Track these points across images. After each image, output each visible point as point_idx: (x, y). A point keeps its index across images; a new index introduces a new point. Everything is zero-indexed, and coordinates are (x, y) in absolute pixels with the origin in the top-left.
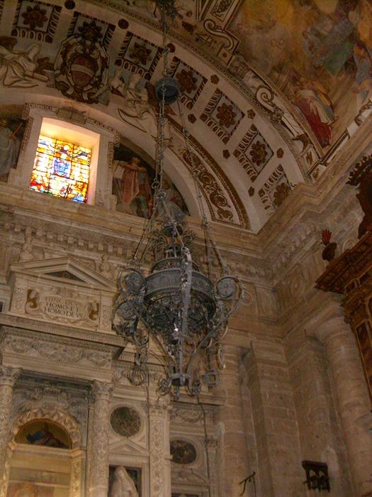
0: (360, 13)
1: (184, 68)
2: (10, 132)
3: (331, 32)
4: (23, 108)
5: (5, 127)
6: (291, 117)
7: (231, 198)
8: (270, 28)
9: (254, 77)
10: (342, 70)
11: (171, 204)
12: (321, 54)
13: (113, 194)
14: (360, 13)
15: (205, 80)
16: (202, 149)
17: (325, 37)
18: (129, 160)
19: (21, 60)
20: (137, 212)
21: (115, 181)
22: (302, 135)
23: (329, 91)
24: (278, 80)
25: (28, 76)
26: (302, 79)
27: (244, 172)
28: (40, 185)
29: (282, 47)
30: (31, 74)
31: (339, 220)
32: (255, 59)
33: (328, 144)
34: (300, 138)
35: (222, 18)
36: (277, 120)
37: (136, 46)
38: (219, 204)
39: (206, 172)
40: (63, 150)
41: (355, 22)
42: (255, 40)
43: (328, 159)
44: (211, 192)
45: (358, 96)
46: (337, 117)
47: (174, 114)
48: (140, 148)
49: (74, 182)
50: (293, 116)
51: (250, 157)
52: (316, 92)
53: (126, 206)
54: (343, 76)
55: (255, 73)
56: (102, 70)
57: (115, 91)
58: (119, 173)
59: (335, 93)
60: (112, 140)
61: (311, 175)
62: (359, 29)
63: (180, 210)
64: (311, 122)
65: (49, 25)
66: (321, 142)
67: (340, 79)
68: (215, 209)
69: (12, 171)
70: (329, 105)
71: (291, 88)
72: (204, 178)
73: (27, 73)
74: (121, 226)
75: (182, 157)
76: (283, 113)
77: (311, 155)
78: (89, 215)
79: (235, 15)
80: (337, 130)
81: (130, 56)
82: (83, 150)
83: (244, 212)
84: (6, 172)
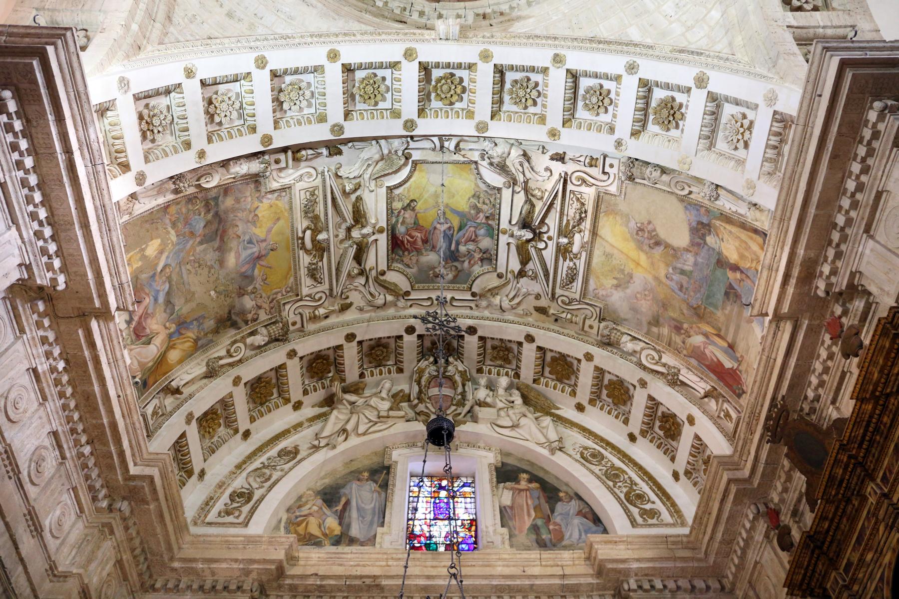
0: (718, 235)
1: (553, 354)
2: (374, 486)
3: (696, 264)
4: (385, 452)
5: (367, 480)
7: (653, 491)
8: (629, 282)
9: (631, 340)
10: (724, 302)
11: (577, 521)
13: (502, 526)
14: (718, 235)
15: (579, 361)
16: (602, 440)
17: (691, 272)
18: (516, 480)
19: (374, 401)
20: (538, 543)
21: (503, 511)
23: (719, 330)
24: (659, 335)
25: (383, 417)
26: (685, 326)
27: (660, 453)
28: (420, 536)
30: (385, 414)
31: (785, 490)
32: (625, 320)
33: (744, 392)
35: (574, 290)
36: (675, 381)
37: (494, 348)
38: (638, 502)
39: (613, 466)
40: (441, 488)
41: (716, 247)
42: (617, 300)
44: (625, 490)
47: (558, 409)
48: (528, 461)
49: (459, 523)
51: (661, 433)
52: (706, 335)
53: (524, 537)
54: (729, 308)
56: (464, 385)
57: (482, 404)
58: (507, 498)
59: (727, 329)
60: (492, 461)
63: (591, 524)
64: (714, 371)
65: (396, 357)
66: (734, 392)
67: (727, 312)
68: (635, 511)
69: (380, 530)
70: (726, 345)
71: (677, 339)
72: (612, 476)
73: (383, 414)
74: (512, 568)
75: (578, 457)
76: (679, 371)
77: (728, 411)
78: (470, 564)
79: (586, 281)
80: (746, 371)
81: (491, 360)
82: (464, 480)
83: (674, 504)
84: (373, 534)
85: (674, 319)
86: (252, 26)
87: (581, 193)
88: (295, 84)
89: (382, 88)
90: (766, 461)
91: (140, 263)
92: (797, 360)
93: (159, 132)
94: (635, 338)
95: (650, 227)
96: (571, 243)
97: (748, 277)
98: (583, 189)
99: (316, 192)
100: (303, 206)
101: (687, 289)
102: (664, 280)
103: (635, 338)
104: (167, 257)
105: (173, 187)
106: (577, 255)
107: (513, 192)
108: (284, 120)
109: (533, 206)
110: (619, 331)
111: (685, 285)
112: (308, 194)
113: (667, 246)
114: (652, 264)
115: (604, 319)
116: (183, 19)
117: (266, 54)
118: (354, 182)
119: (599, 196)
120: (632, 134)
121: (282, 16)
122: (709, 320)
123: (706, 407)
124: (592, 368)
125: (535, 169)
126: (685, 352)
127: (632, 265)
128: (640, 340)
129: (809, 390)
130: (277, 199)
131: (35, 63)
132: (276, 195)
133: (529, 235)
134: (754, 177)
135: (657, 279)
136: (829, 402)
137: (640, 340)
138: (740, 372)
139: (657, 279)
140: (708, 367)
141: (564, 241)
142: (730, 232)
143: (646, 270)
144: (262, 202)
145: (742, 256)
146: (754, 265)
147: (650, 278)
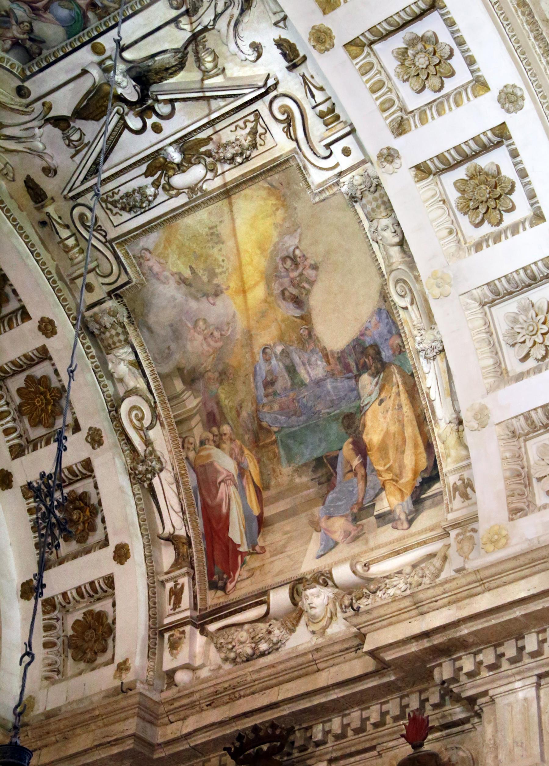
0: (381, 390)
3: (319, 383)
6: (174, 487)
8: (206, 295)
9: (131, 363)
12: (282, 408)
14: (381, 390)
17: (303, 384)
22: (179, 537)
26: (226, 429)
27: (31, 538)
29: (212, 343)
33: (224, 588)
34: (172, 539)
35: (117, 220)
41: (366, 400)
43: (211, 622)
45: (316, 537)
46: (263, 548)
50: (178, 487)
52: (242, 471)
54: (305, 479)
55: (137, 356)
61: (166, 635)
62: (369, 414)
64: (207, 521)
66: (211, 574)
67: (297, 480)
70: (256, 512)
76: (161, 470)
80: (252, 573)
85: (218, 403)
87: (267, 129)
90: (196, 745)
92: (343, 697)
94: (138, 364)
95: (310, 273)
96: (180, 168)
97: (365, 478)
98: (277, 130)
101: (275, 393)
102: (257, 350)
103: (138, 364)
106: (172, 188)
107: (175, 21)
109: (181, 66)
110: (126, 333)
111: (279, 386)
113: (306, 319)
114: (263, 314)
115: (118, 296)
119: (287, 161)
120: (418, 167)
122: (265, 459)
123: (156, 554)
124: (38, 344)
125: (240, 28)
126: (192, 455)
127: (233, 284)
128: (144, 375)
129: (320, 727)
133: (132, 95)
134: (497, 416)
135: (249, 336)
136: (328, 757)
137: (144, 375)
138: (243, 562)
139: (249, 336)
140: (205, 508)
141: (176, 156)
142: (400, 407)
143: (247, 310)
145: (383, 448)
146: (387, 476)
147: (240, 325)
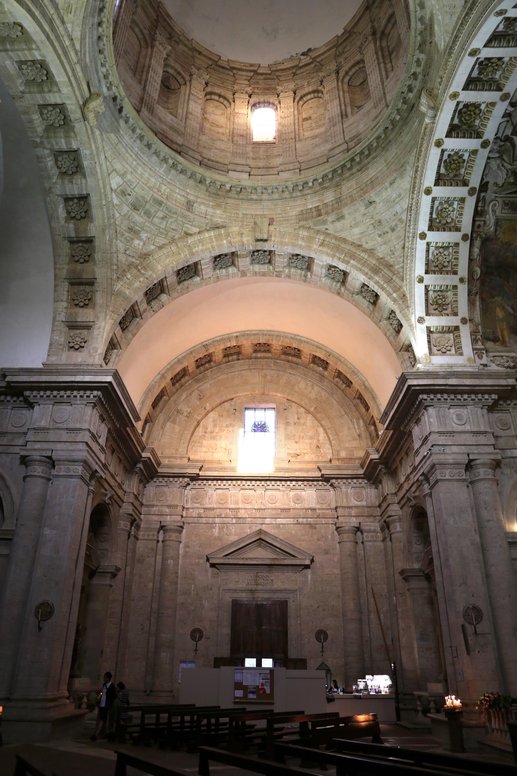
86: (400, 220)
88: (438, 213)
89: (455, 158)
91: (505, 323)
93: (444, 301)
99: (506, 202)
100: (512, 212)
104: (508, 305)
105: (473, 296)
108: (456, 222)
112: (505, 207)
116: (391, 258)
117: (419, 232)
118: (510, 175)
121: (398, 200)
130: (501, 228)
131: (413, 388)
132: (498, 228)
144: (499, 238)
